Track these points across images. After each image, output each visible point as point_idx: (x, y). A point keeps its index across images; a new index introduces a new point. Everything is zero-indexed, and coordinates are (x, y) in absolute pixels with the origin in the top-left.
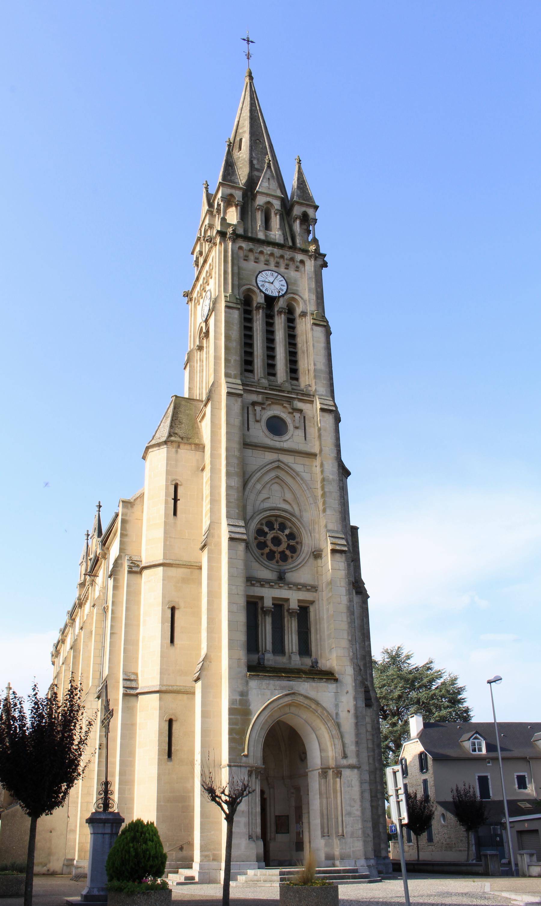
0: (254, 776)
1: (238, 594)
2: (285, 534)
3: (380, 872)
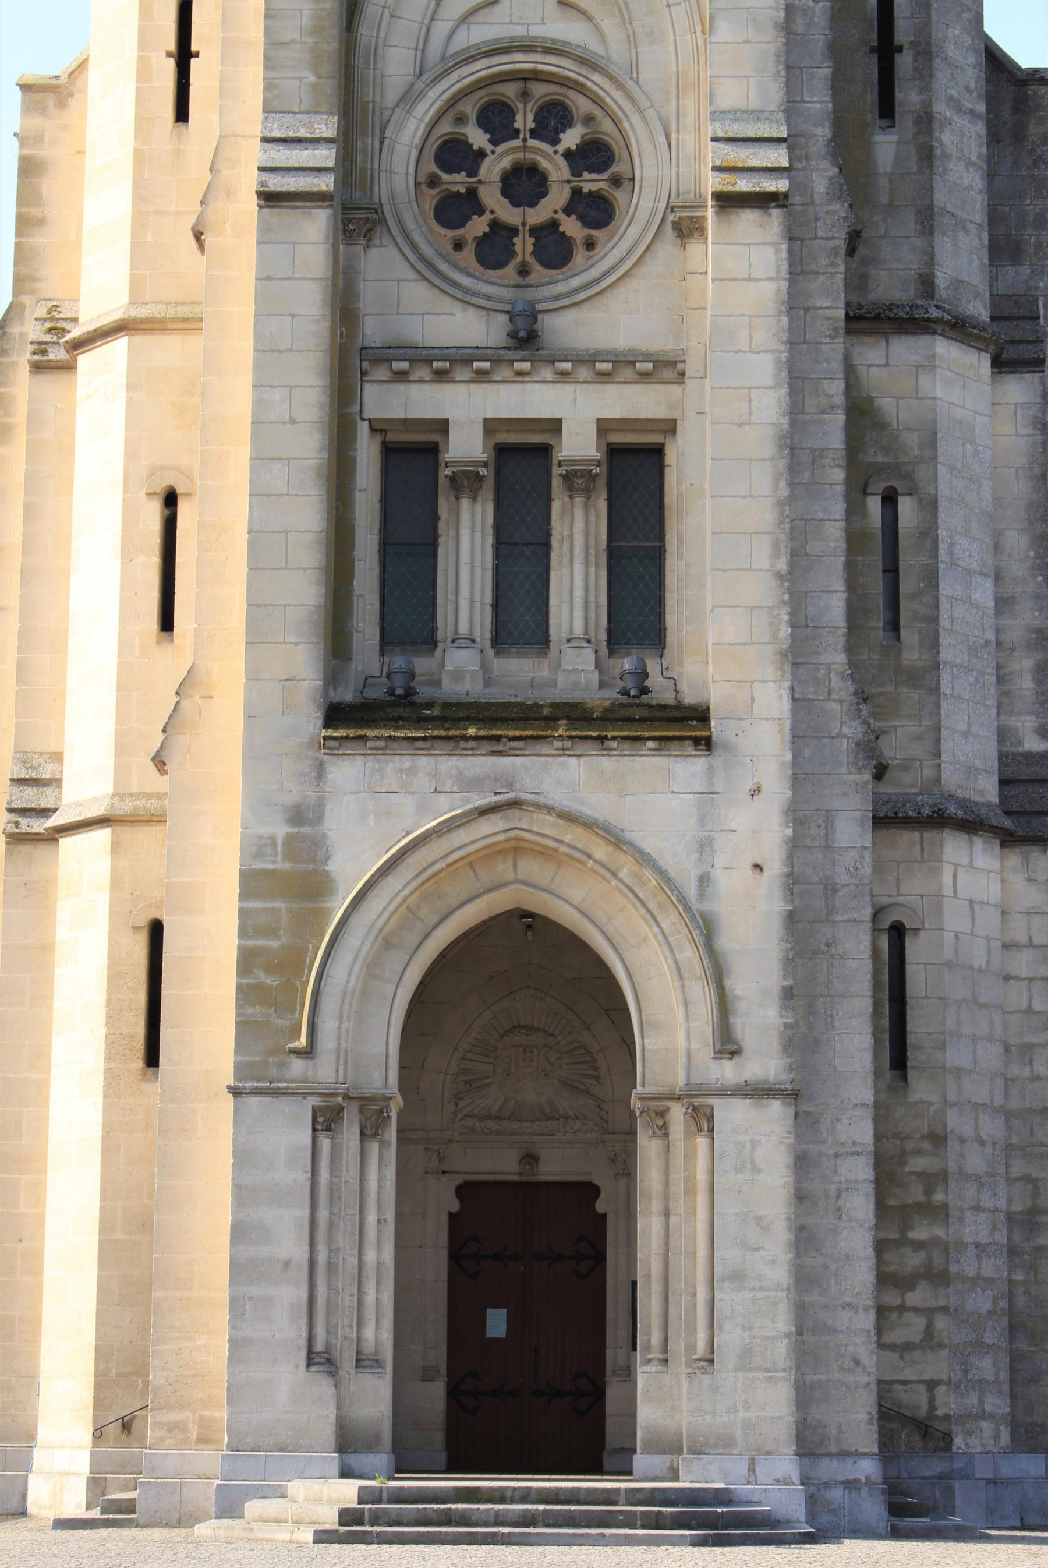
0: (350, 1132)
1: (293, 421)
2: (561, 148)
3: (896, 1510)
